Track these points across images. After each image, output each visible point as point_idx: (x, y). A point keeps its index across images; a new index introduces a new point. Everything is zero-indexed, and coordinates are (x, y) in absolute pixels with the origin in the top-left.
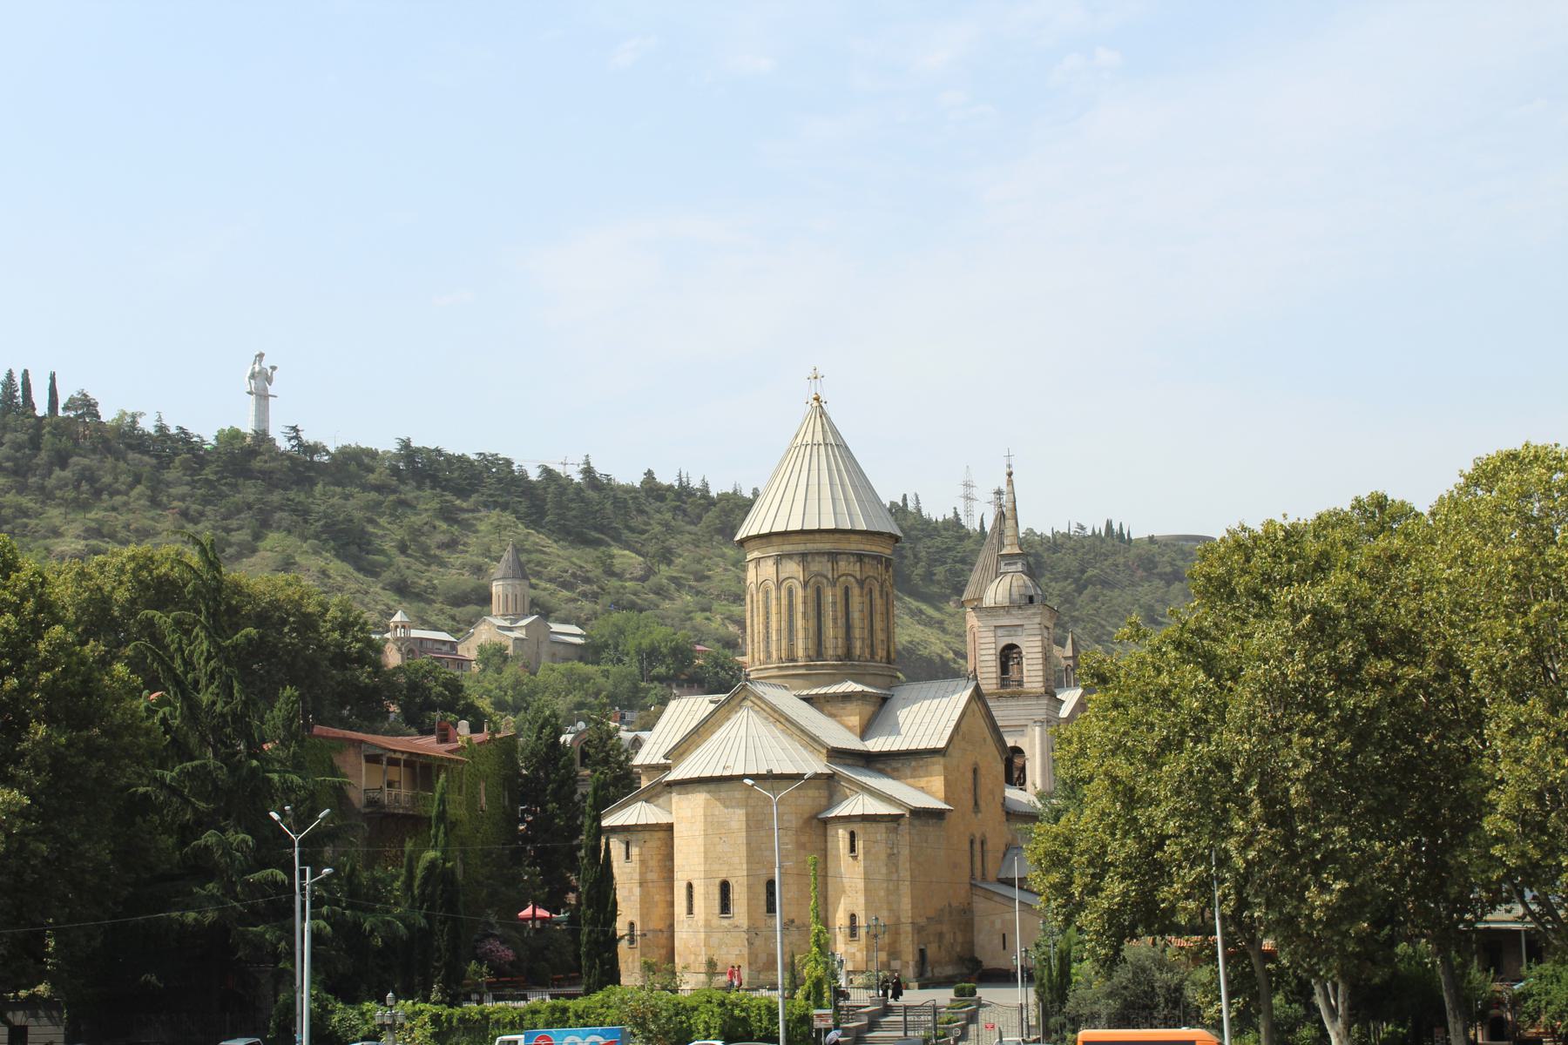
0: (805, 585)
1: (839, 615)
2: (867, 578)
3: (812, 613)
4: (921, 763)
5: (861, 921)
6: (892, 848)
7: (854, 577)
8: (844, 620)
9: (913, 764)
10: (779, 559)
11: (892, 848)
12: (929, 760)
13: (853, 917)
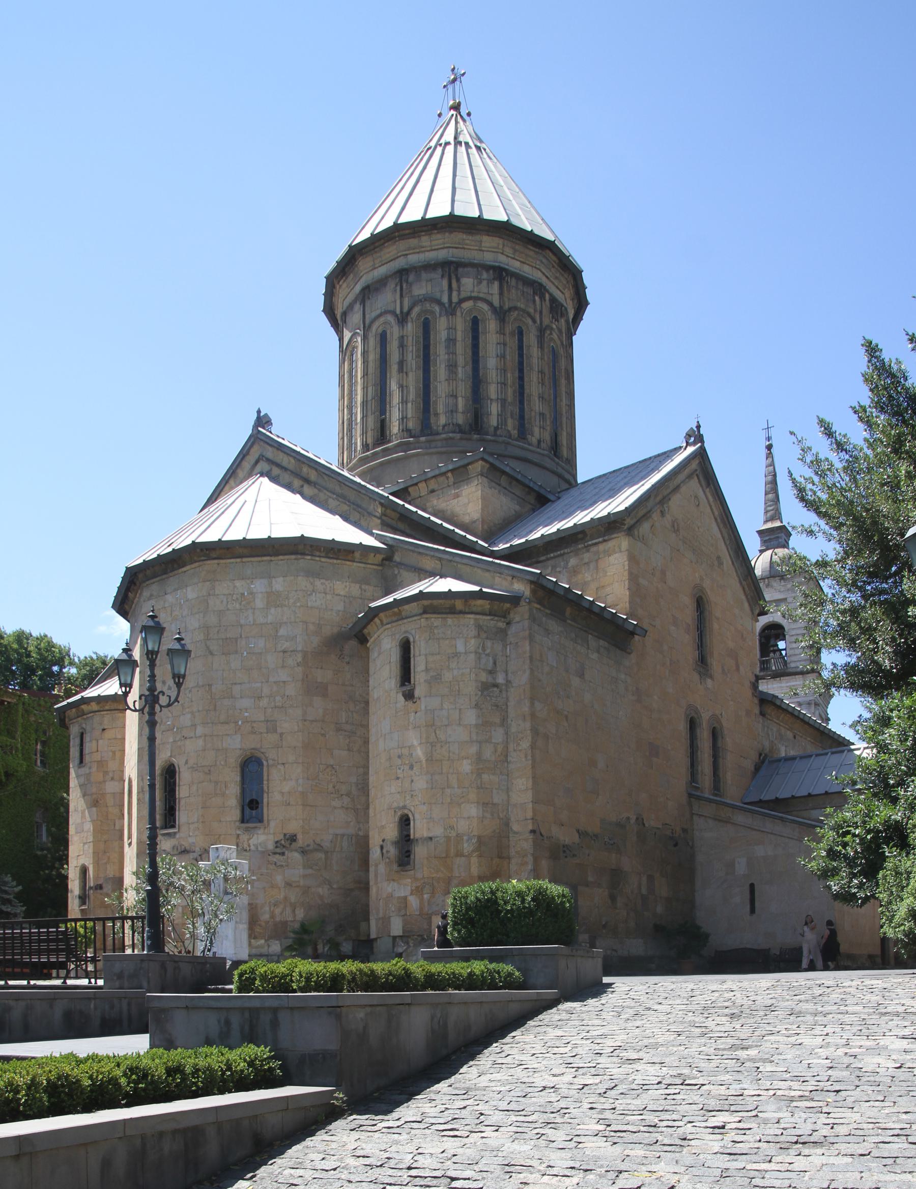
0: (402, 319)
1: (461, 360)
2: (510, 309)
3: (412, 361)
4: (586, 556)
5: (419, 829)
6: (491, 672)
7: (490, 304)
8: (469, 369)
9: (573, 562)
10: (367, 292)
11: (491, 672)
12: (601, 547)
13: (405, 822)
